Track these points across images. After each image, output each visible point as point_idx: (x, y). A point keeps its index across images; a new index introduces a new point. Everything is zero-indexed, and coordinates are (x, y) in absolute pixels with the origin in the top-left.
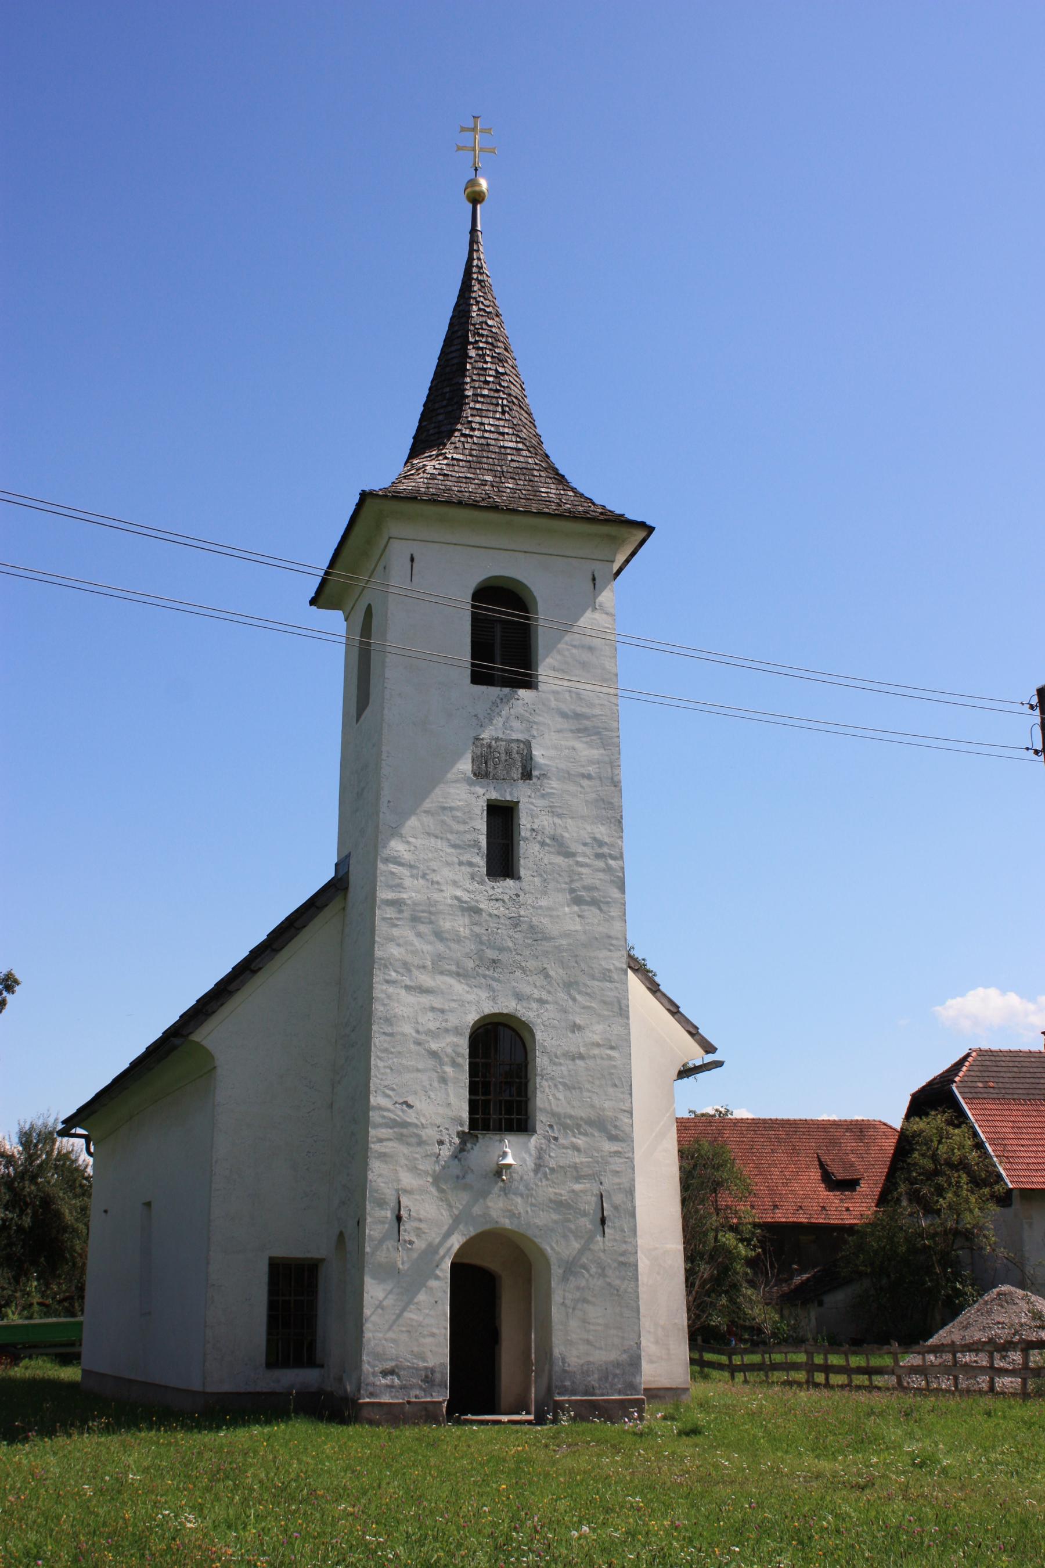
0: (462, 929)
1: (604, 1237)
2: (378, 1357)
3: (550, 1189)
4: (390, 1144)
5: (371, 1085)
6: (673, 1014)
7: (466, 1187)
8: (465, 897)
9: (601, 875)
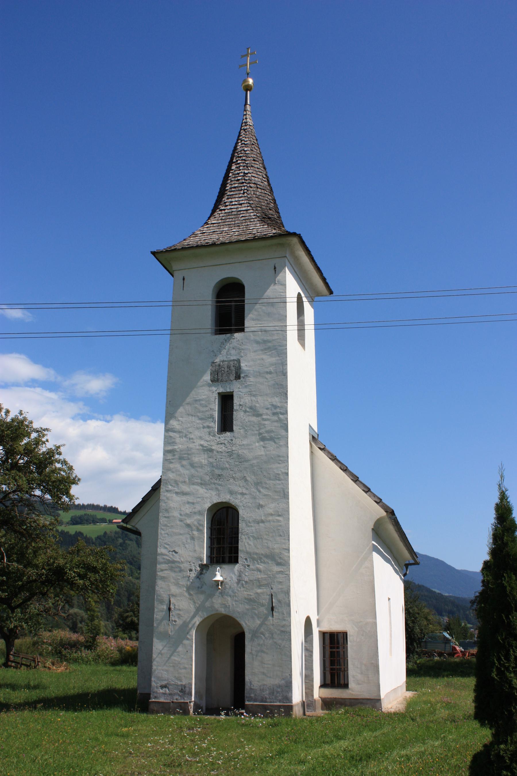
0: (203, 461)
1: (273, 617)
2: (159, 678)
3: (245, 592)
4: (166, 572)
5: (158, 543)
6: (366, 492)
7: (203, 593)
8: (205, 444)
9: (276, 424)
